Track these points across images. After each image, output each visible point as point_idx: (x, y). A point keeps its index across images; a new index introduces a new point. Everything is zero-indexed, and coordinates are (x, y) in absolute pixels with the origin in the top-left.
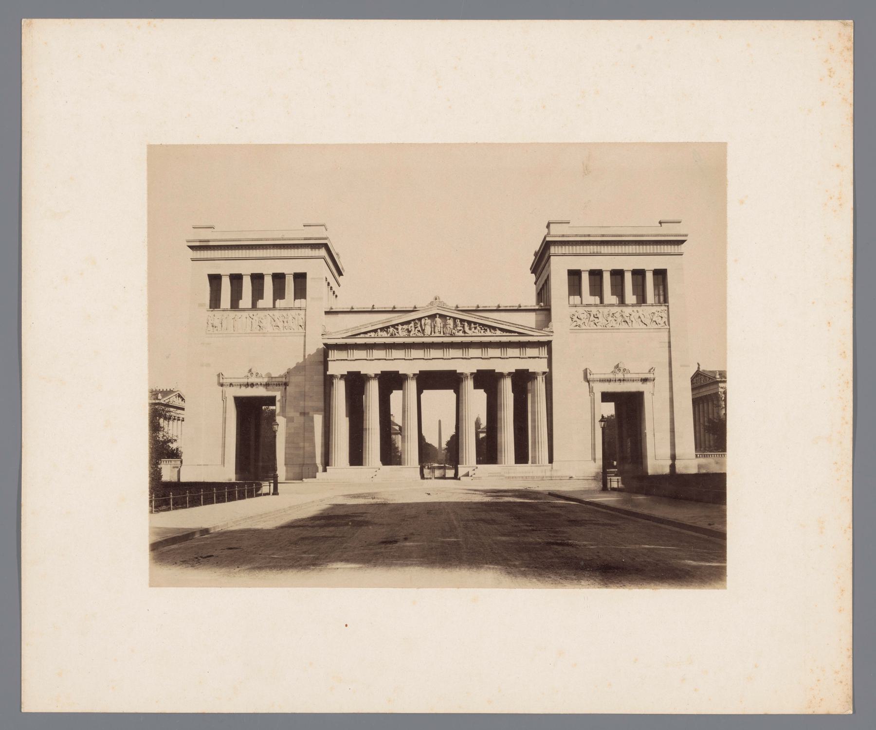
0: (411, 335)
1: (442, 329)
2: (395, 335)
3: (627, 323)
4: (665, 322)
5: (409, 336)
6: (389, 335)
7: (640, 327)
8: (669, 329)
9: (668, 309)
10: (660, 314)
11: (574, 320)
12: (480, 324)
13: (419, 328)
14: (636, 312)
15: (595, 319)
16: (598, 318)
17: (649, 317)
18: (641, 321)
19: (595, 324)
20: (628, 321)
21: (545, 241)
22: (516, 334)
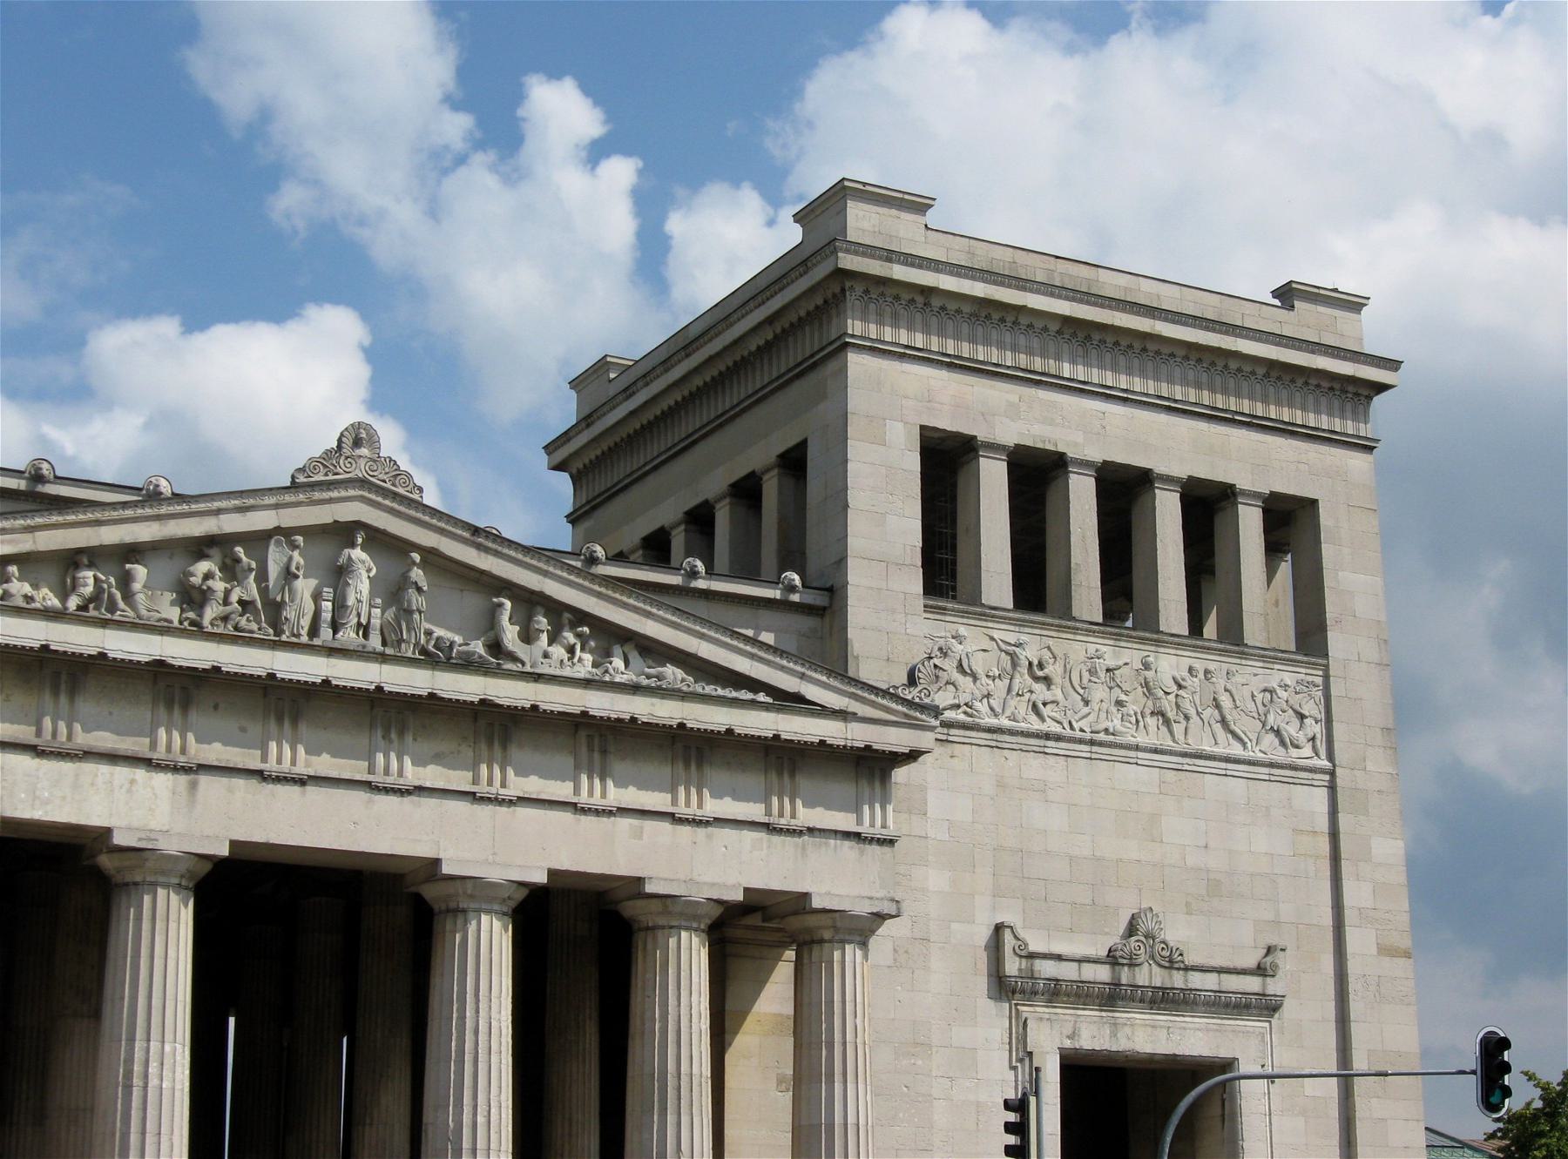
0: (206, 622)
1: (377, 612)
2: (112, 607)
3: (1167, 722)
4: (1313, 739)
5: (196, 631)
6: (73, 603)
7: (1218, 750)
8: (1332, 774)
9: (1326, 677)
10: (1295, 700)
11: (944, 676)
12: (581, 617)
13: (251, 590)
14: (1201, 675)
16: (1047, 680)
17: (1251, 706)
18: (1223, 722)
19: (1035, 707)
20: (1171, 714)
21: (819, 272)
22: (762, 697)
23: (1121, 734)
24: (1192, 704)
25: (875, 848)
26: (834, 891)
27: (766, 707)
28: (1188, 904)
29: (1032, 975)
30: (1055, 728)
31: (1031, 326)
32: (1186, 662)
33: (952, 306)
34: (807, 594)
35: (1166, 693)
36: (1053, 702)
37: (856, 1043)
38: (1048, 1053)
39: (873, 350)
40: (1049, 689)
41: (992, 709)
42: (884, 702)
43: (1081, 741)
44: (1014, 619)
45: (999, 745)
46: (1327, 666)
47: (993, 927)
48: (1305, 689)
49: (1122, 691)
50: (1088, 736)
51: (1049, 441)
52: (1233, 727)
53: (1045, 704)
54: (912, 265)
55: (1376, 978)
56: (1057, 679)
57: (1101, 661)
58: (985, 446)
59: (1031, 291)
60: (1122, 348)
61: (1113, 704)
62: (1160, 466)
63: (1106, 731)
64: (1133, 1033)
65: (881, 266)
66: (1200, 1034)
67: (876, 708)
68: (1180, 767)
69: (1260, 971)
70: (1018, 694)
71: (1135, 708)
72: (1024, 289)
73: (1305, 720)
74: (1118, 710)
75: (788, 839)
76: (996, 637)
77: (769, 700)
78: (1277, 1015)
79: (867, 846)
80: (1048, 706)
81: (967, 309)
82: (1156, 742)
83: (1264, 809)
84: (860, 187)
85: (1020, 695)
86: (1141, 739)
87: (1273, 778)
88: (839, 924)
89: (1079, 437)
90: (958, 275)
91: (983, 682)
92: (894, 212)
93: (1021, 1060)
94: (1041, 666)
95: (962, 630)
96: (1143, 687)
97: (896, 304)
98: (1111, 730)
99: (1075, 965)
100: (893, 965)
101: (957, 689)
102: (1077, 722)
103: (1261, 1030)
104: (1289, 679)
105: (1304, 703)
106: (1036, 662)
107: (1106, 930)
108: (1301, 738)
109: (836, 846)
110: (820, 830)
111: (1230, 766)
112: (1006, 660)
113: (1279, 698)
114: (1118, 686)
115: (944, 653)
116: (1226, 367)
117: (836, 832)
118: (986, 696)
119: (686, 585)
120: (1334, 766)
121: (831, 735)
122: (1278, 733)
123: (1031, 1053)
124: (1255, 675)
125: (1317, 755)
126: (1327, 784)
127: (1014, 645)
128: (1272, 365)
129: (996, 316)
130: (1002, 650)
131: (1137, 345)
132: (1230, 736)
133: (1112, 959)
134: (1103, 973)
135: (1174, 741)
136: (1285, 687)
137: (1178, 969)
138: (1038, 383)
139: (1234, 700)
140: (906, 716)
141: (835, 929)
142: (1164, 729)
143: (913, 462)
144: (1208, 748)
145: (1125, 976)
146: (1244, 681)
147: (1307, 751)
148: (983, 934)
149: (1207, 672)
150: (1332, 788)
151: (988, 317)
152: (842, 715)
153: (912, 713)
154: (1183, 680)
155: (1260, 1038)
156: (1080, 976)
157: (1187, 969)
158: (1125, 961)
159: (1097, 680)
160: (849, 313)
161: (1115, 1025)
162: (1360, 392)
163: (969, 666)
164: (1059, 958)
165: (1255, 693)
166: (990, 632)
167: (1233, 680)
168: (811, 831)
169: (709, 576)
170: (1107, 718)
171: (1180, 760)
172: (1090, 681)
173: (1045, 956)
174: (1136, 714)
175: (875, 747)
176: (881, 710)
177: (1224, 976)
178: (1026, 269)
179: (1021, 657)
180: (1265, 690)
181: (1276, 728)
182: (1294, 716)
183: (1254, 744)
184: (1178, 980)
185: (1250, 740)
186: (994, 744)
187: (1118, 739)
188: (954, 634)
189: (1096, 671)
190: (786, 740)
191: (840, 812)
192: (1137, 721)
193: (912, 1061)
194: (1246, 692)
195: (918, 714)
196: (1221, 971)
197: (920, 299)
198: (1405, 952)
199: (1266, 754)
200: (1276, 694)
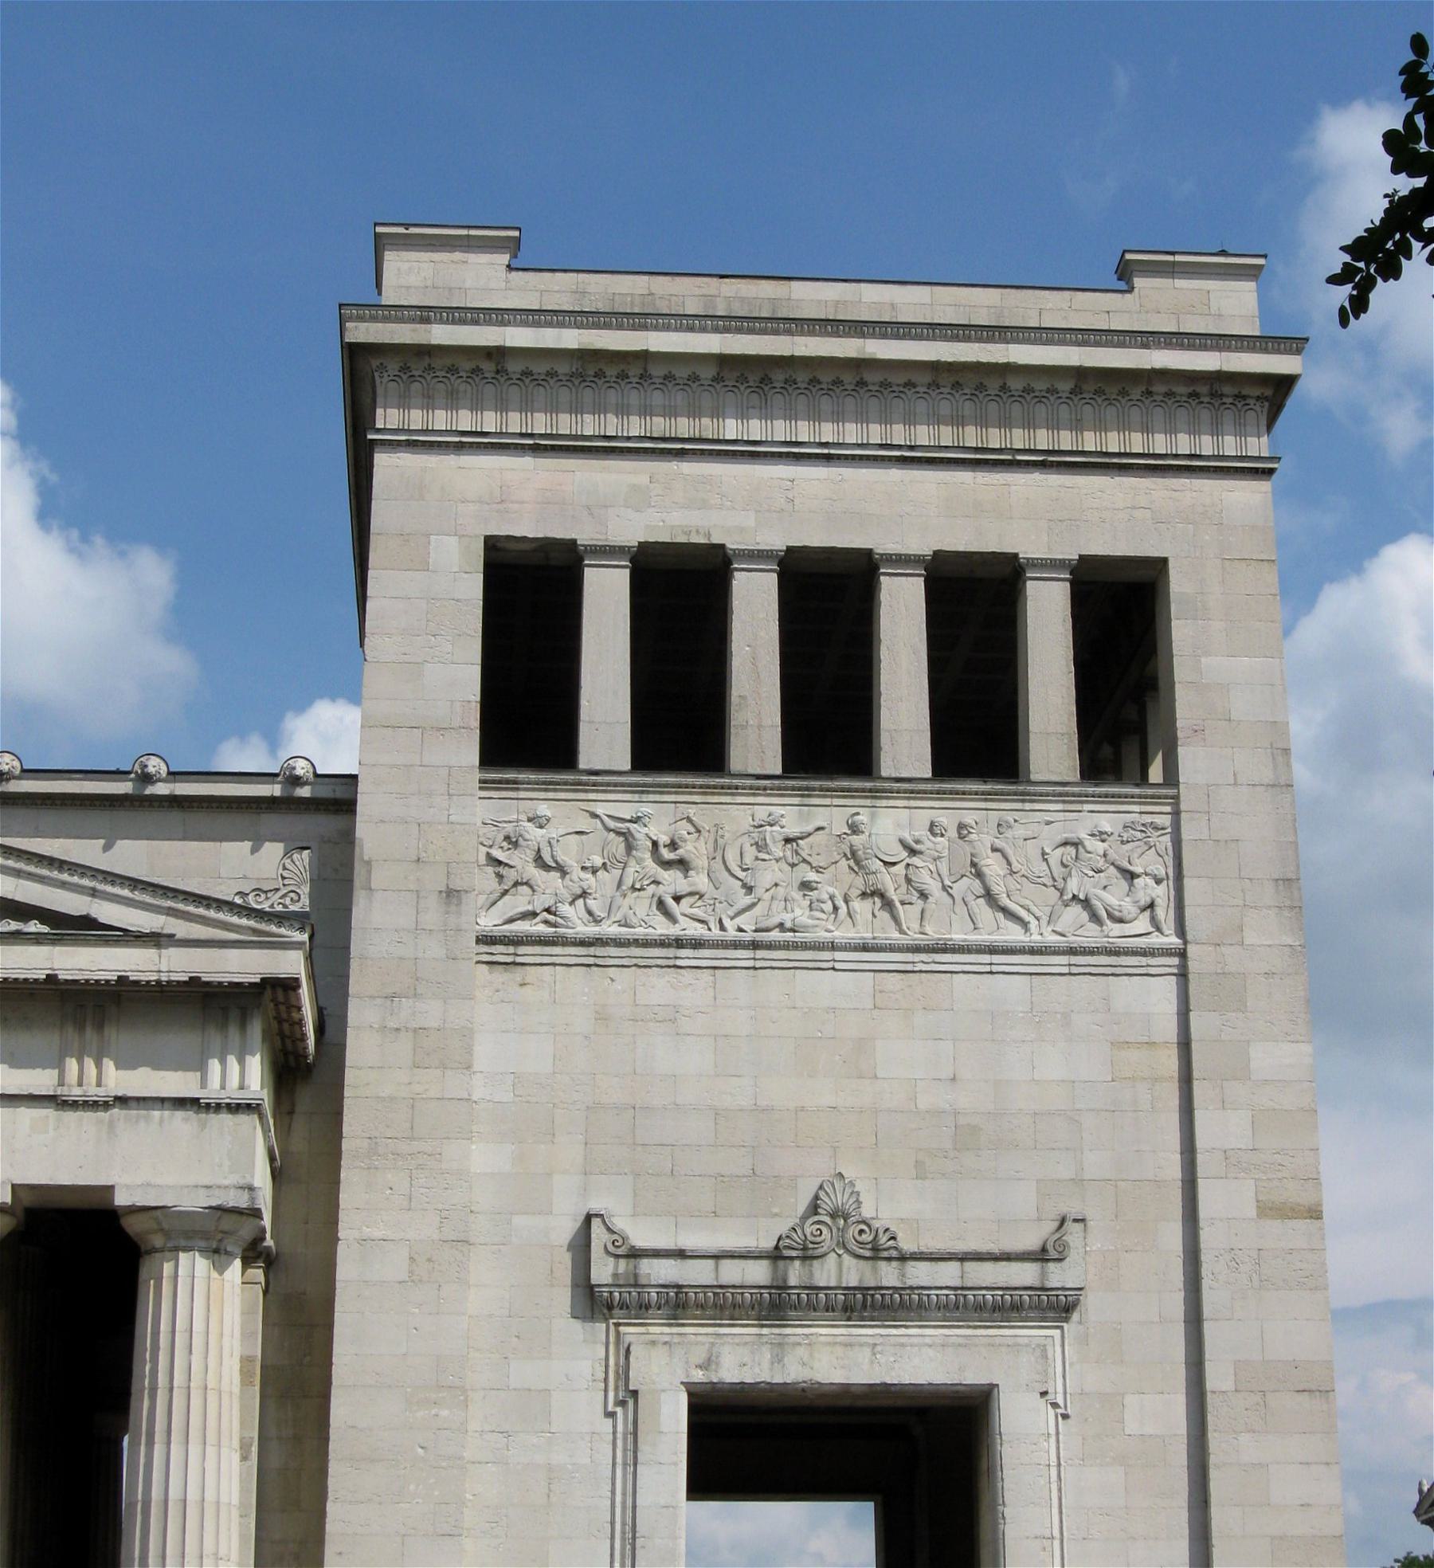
3: (888, 905)
4: (1151, 906)
8: (1183, 954)
9: (1176, 814)
10: (1119, 854)
11: (511, 875)
14: (953, 833)
15: (666, 876)
16: (683, 864)
18: (989, 896)
19: (661, 904)
22: (34, 927)
23: (805, 928)
24: (935, 875)
25: (226, 1118)
26: (159, 1181)
27: (37, 939)
28: (918, 1164)
29: (636, 1281)
30: (695, 930)
31: (669, 377)
32: (924, 817)
33: (539, 368)
34: (322, 784)
35: (885, 863)
36: (691, 894)
37: (189, 1387)
38: (663, 1391)
39: (412, 445)
40: (686, 877)
41: (590, 913)
42: (221, 916)
43: (736, 945)
44: (630, 785)
45: (599, 961)
46: (1177, 797)
47: (583, 1218)
48: (1139, 835)
49: (812, 867)
50: (748, 937)
51: (697, 531)
52: (1005, 901)
53: (677, 899)
54: (463, 322)
55: (1254, 1254)
56: (700, 861)
57: (776, 828)
58: (591, 552)
59: (656, 328)
60: (824, 386)
61: (796, 885)
62: (882, 543)
63: (781, 926)
64: (811, 1355)
65: (414, 330)
66: (931, 1352)
67: (208, 925)
68: (909, 967)
69: (1041, 1256)
70: (633, 889)
71: (831, 890)
72: (644, 327)
73: (1136, 881)
74: (805, 895)
75: (89, 1116)
76: (599, 811)
77: (45, 929)
78: (1075, 1316)
79: (212, 1116)
80: (684, 901)
81: (563, 368)
82: (865, 935)
83: (1059, 1016)
84: (401, 230)
85: (639, 890)
86: (842, 934)
87: (1075, 970)
88: (166, 1226)
89: (749, 520)
90: (537, 324)
91: (575, 878)
92: (458, 256)
93: (622, 1403)
94: (673, 845)
95: (543, 809)
96: (848, 859)
97: (453, 378)
98: (788, 925)
99: (711, 1263)
100: (407, 1279)
101: (534, 891)
102: (732, 918)
103: (1042, 1341)
104: (1106, 823)
105: (1136, 855)
106: (664, 839)
107: (776, 1210)
108: (1128, 907)
109: (161, 1117)
110: (138, 1099)
111: (996, 959)
112: (618, 845)
113: (1089, 853)
114: (804, 861)
115: (513, 842)
116: (1004, 388)
117: (163, 1100)
118: (580, 896)
119: (137, 793)
120: (1185, 943)
121: (134, 967)
122: (1086, 903)
123: (635, 1393)
124: (1048, 823)
125: (1159, 929)
126: (1175, 971)
127: (630, 821)
128: (1081, 374)
129: (611, 372)
130: (610, 830)
131: (848, 378)
132: (1000, 915)
133: (776, 1256)
134: (758, 1273)
135: (902, 932)
136: (1102, 836)
137: (889, 1259)
138: (681, 454)
139: (1009, 863)
140: (255, 931)
141: (167, 1234)
142: (885, 916)
143: (472, 588)
144: (959, 935)
145: (795, 1274)
146: (1030, 834)
147: (1142, 924)
148: (565, 1228)
149: (961, 826)
150: (1183, 975)
151: (600, 374)
152: (155, 939)
153: (263, 926)
154: (917, 842)
155: (1038, 1352)
156: (717, 1278)
157: (903, 1258)
158: (794, 1253)
159: (767, 857)
160: (380, 400)
161: (780, 1348)
162: (1244, 392)
163: (553, 857)
164: (681, 1254)
165: (1047, 850)
166: (592, 807)
167: (1009, 834)
168: (122, 1101)
169: (172, 777)
170: (785, 909)
171: (909, 957)
172: (757, 859)
173: (657, 1254)
174: (832, 898)
175: (205, 978)
176: (215, 927)
177: (969, 1265)
178: (670, 300)
179: (637, 835)
180: (1065, 844)
181: (1082, 897)
182: (1119, 876)
183: (1044, 922)
184: (888, 1275)
185: (1038, 919)
186: (591, 961)
187: (799, 937)
188: (530, 815)
189: (766, 845)
190: (66, 980)
191: (134, 1068)
192: (836, 908)
193: (433, 1412)
194: (1033, 850)
195: (273, 928)
196: (963, 1258)
197: (488, 367)
198: (1310, 1210)
199: (1064, 936)
200: (1084, 847)
